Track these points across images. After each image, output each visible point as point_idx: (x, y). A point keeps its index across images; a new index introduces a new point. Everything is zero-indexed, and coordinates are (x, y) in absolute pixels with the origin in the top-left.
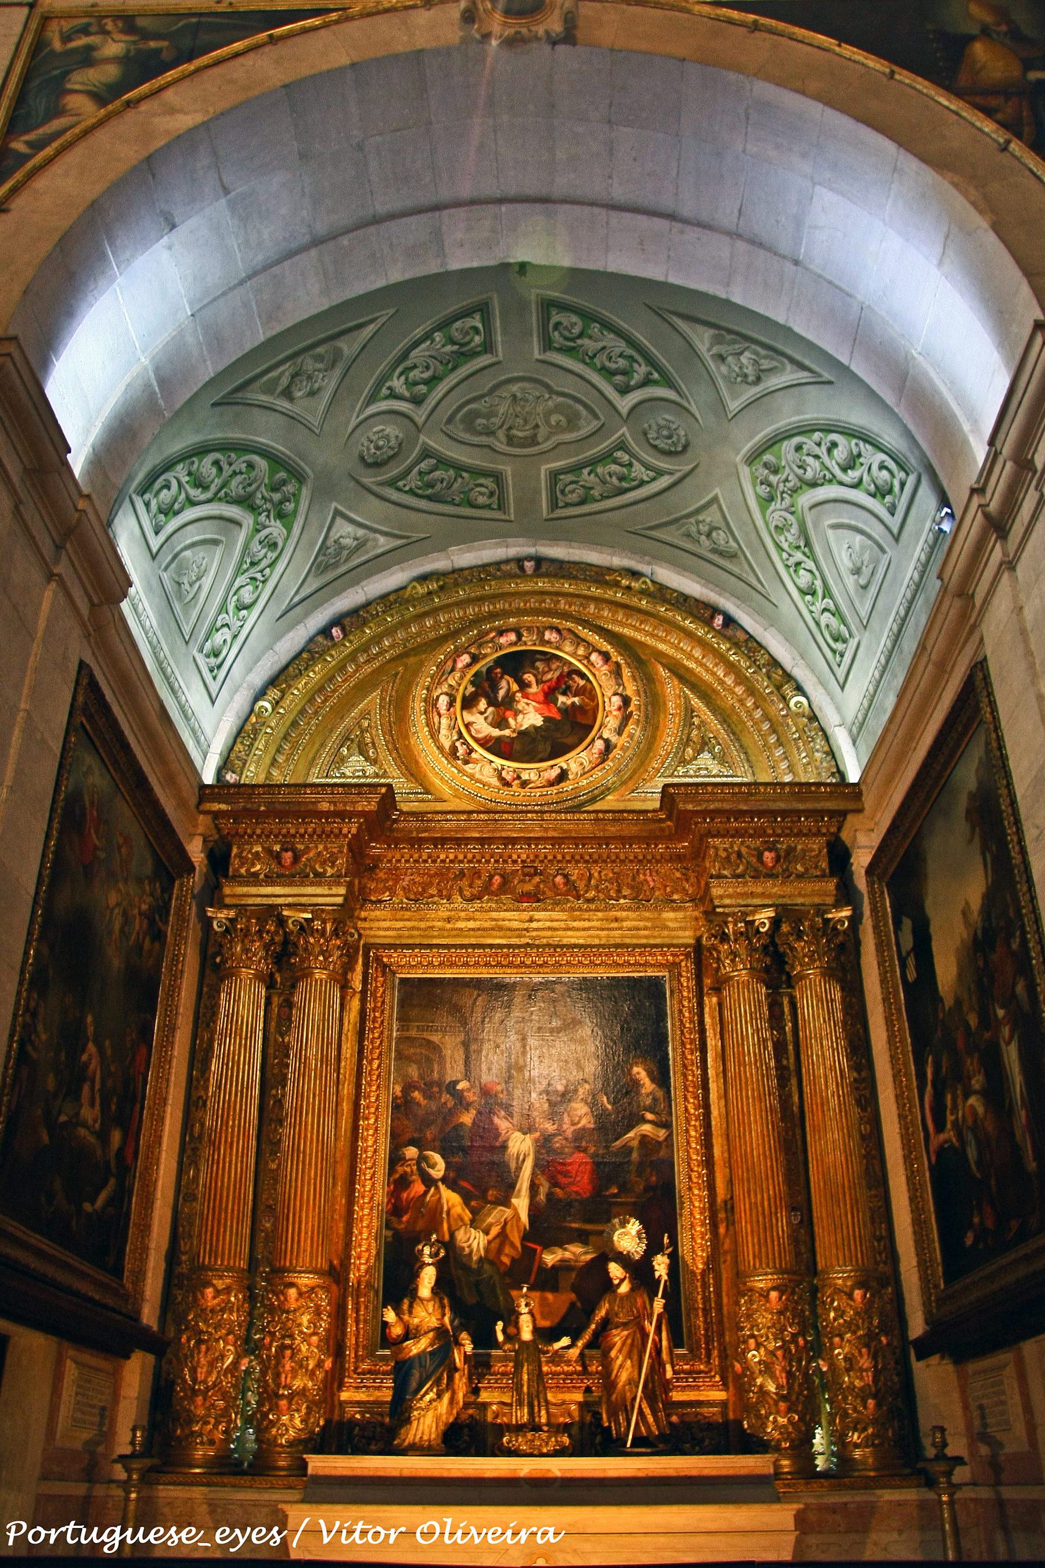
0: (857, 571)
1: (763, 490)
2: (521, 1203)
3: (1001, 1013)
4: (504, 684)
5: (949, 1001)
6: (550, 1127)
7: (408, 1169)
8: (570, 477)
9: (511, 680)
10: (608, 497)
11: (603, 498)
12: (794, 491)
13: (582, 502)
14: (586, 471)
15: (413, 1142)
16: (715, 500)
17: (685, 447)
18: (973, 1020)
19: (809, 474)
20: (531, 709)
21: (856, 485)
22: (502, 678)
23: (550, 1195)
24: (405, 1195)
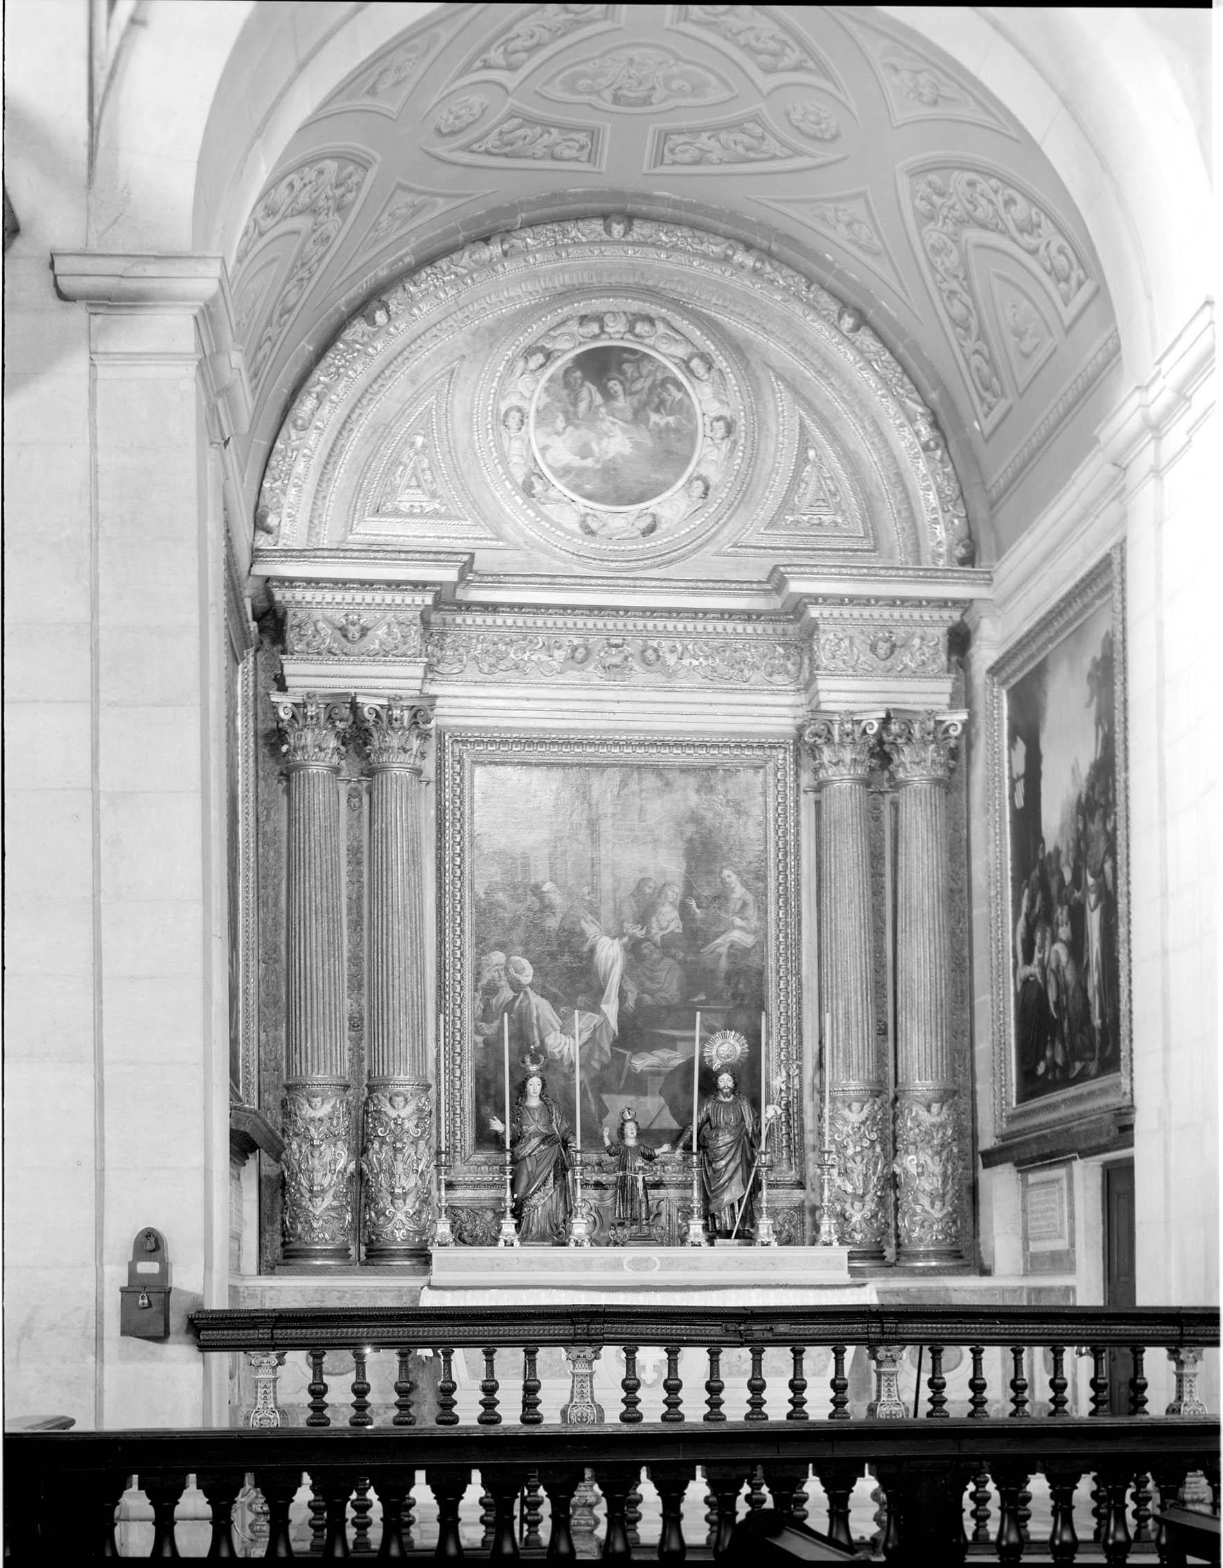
0: (1019, 334)
1: (923, 206)
2: (610, 1009)
3: (1091, 881)
4: (584, 394)
5: (1049, 847)
6: (639, 933)
7: (496, 975)
8: (683, 139)
9: (593, 388)
10: (728, 163)
11: (721, 162)
12: (960, 222)
13: (696, 162)
14: (705, 135)
15: (502, 946)
16: (862, 195)
17: (834, 138)
18: (1068, 876)
19: (979, 214)
20: (618, 431)
21: (1033, 252)
22: (582, 385)
23: (638, 1001)
24: (494, 1001)
